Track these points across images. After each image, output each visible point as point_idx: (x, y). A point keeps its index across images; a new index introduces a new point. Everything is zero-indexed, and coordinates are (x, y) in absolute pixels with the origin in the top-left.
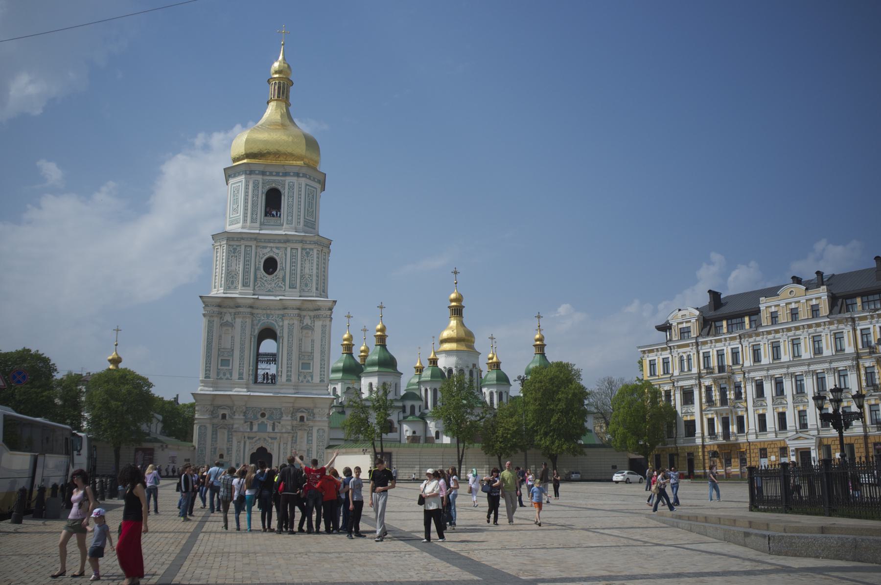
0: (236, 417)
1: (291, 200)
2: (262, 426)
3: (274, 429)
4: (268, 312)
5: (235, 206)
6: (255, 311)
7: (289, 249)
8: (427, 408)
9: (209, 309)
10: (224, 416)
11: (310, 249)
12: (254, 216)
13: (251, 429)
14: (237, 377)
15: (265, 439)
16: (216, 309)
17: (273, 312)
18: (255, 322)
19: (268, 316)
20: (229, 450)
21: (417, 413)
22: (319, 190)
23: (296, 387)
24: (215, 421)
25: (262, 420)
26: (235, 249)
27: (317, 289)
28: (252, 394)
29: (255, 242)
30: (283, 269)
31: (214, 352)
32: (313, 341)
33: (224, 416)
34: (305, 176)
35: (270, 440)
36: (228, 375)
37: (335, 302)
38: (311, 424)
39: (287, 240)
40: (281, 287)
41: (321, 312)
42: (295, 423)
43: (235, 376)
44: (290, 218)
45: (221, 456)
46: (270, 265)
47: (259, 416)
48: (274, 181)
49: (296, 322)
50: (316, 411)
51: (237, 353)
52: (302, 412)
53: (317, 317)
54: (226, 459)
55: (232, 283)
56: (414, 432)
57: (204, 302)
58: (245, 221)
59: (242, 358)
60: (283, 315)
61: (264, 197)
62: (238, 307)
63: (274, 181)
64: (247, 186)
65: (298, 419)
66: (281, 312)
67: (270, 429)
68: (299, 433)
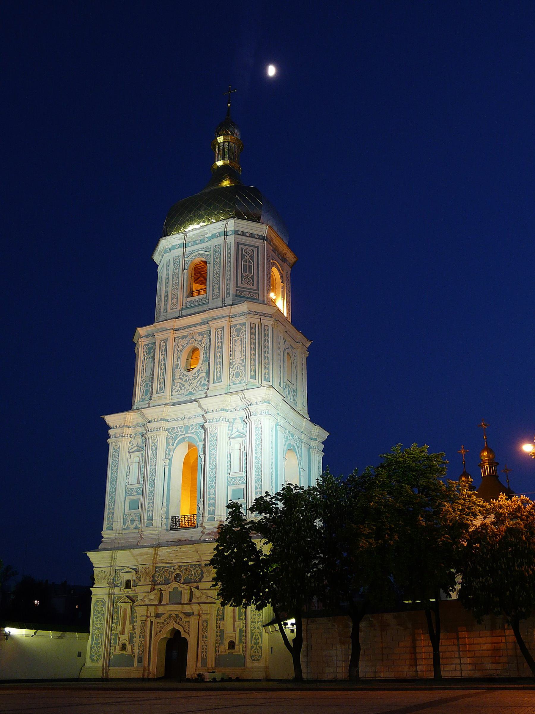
11: (241, 325)
13: (161, 601)
15: (177, 616)
17: (191, 422)
25: (175, 585)
44: (216, 290)
67: (185, 598)
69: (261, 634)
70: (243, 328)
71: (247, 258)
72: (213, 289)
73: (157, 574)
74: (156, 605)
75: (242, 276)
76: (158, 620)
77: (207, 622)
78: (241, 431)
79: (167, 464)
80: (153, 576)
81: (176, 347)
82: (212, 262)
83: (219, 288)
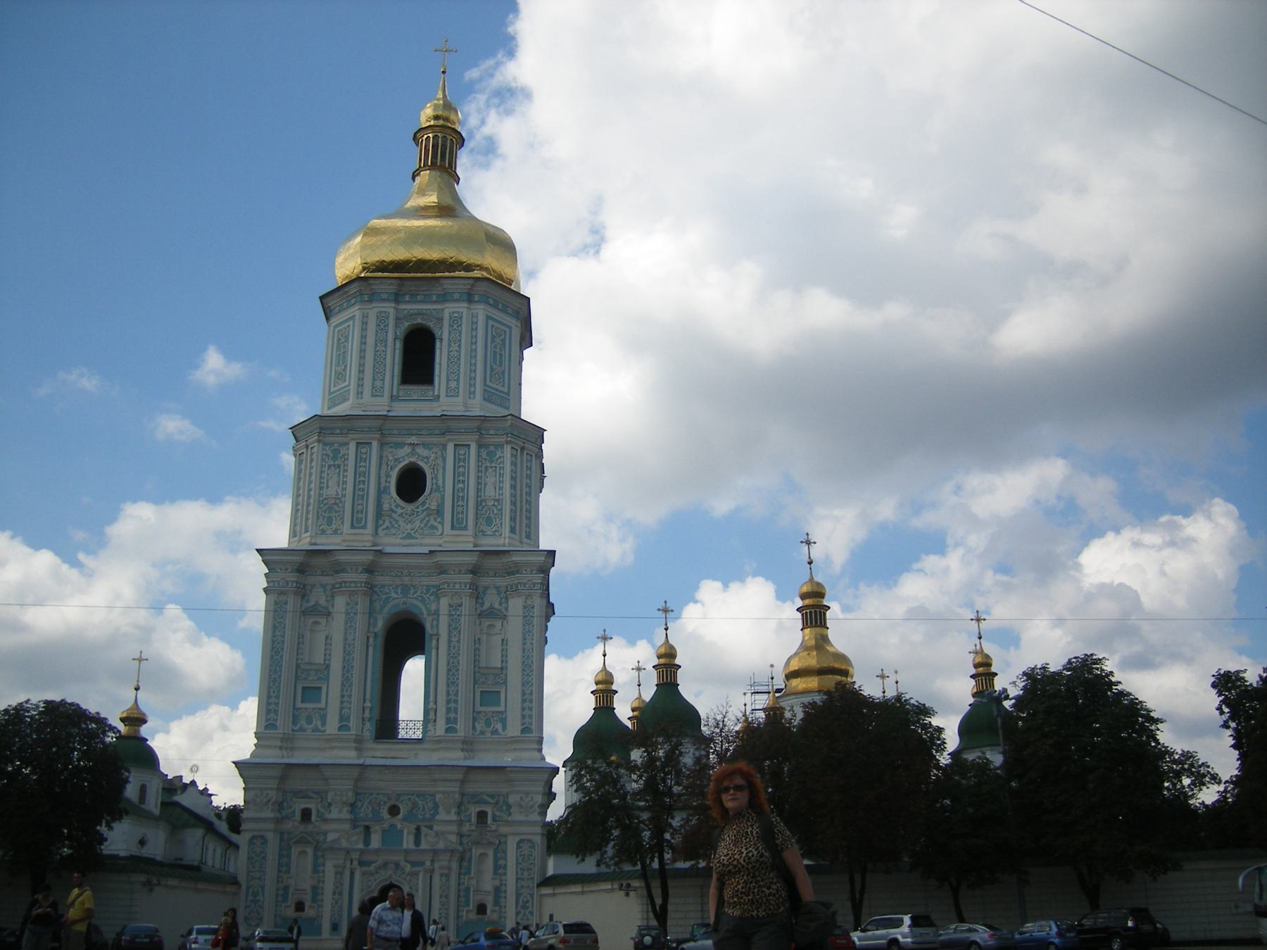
0: (334, 814)
1: (454, 347)
3: (417, 842)
4: (407, 580)
6: (380, 580)
7: (450, 447)
10: (306, 815)
12: (378, 384)
13: (367, 842)
15: (397, 865)
16: (292, 577)
18: (377, 605)
19: (405, 589)
20: (316, 891)
22: (517, 333)
23: (468, 745)
24: (288, 826)
26: (336, 452)
27: (513, 530)
28: (368, 762)
33: (306, 815)
34: (485, 300)
35: (408, 868)
37: (552, 554)
38: (504, 830)
39: (446, 425)
44: (453, 384)
45: (300, 907)
46: (412, 484)
47: (385, 813)
48: (420, 313)
49: (467, 602)
54: (309, 912)
57: (265, 562)
58: (359, 394)
59: (346, 682)
60: (438, 588)
61: (399, 345)
62: (339, 568)
63: (418, 309)
64: (364, 324)
65: (474, 819)
66: (435, 581)
67: (408, 842)
69: (532, 896)
70: (499, 454)
71: (498, 340)
72: (448, 380)
73: (359, 804)
74: (362, 852)
75: (492, 369)
76: (364, 869)
77: (447, 876)
78: (496, 606)
79: (371, 640)
80: (353, 805)
81: (384, 460)
82: (445, 337)
83: (458, 380)
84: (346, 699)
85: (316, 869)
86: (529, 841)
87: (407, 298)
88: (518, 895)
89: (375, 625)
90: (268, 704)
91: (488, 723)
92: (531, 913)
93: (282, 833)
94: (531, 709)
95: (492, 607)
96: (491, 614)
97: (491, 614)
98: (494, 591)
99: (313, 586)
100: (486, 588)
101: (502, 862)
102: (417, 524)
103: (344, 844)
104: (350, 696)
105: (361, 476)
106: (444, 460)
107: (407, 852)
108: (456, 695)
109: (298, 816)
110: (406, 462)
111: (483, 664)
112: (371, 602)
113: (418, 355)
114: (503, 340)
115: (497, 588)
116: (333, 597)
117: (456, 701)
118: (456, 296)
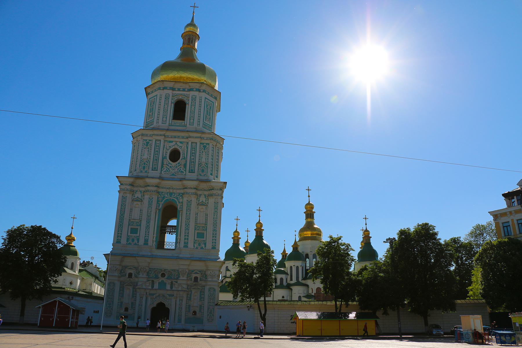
1: (193, 108)
2: (162, 285)
3: (171, 287)
4: (171, 191)
5: (150, 114)
6: (160, 190)
8: (291, 280)
9: (123, 187)
10: (130, 275)
11: (207, 144)
12: (165, 119)
13: (153, 287)
14: (143, 242)
15: (164, 296)
16: (129, 187)
17: (175, 191)
18: (160, 198)
21: (285, 284)
25: (161, 279)
26: (148, 143)
29: (163, 137)
30: (184, 158)
31: (126, 222)
32: (206, 215)
34: (204, 91)
36: (136, 241)
38: (204, 283)
40: (182, 172)
41: (214, 192)
42: (189, 282)
43: (141, 242)
44: (192, 121)
45: (126, 309)
46: (175, 156)
49: (194, 199)
50: (208, 273)
51: (144, 223)
52: (196, 273)
53: (211, 195)
54: (130, 311)
55: (144, 168)
56: (283, 297)
57: (120, 182)
59: (148, 227)
60: (183, 194)
61: (173, 105)
67: (168, 287)
68: (193, 291)
69: (214, 309)
70: (207, 147)
71: (209, 106)
72: (190, 119)
75: (206, 117)
78: (204, 201)
81: (165, 147)
83: (194, 120)
84: (147, 233)
85: (133, 297)
86: (213, 288)
87: (177, 89)
88: (208, 309)
89: (159, 206)
90: (118, 234)
91: (199, 244)
92: (213, 315)
93: (121, 282)
94: (215, 240)
95: (202, 202)
96: (203, 204)
97: (203, 204)
98: (204, 196)
99: (137, 191)
100: (200, 195)
101: (203, 296)
102: (176, 170)
103: (144, 287)
104: (149, 232)
105: (156, 152)
106: (187, 148)
107: (167, 290)
108: (188, 233)
109: (127, 276)
110: (174, 147)
111: (198, 222)
112: (158, 198)
113: (180, 110)
114: (211, 107)
115: (205, 195)
116: (144, 195)
117: (188, 236)
118: (195, 90)
